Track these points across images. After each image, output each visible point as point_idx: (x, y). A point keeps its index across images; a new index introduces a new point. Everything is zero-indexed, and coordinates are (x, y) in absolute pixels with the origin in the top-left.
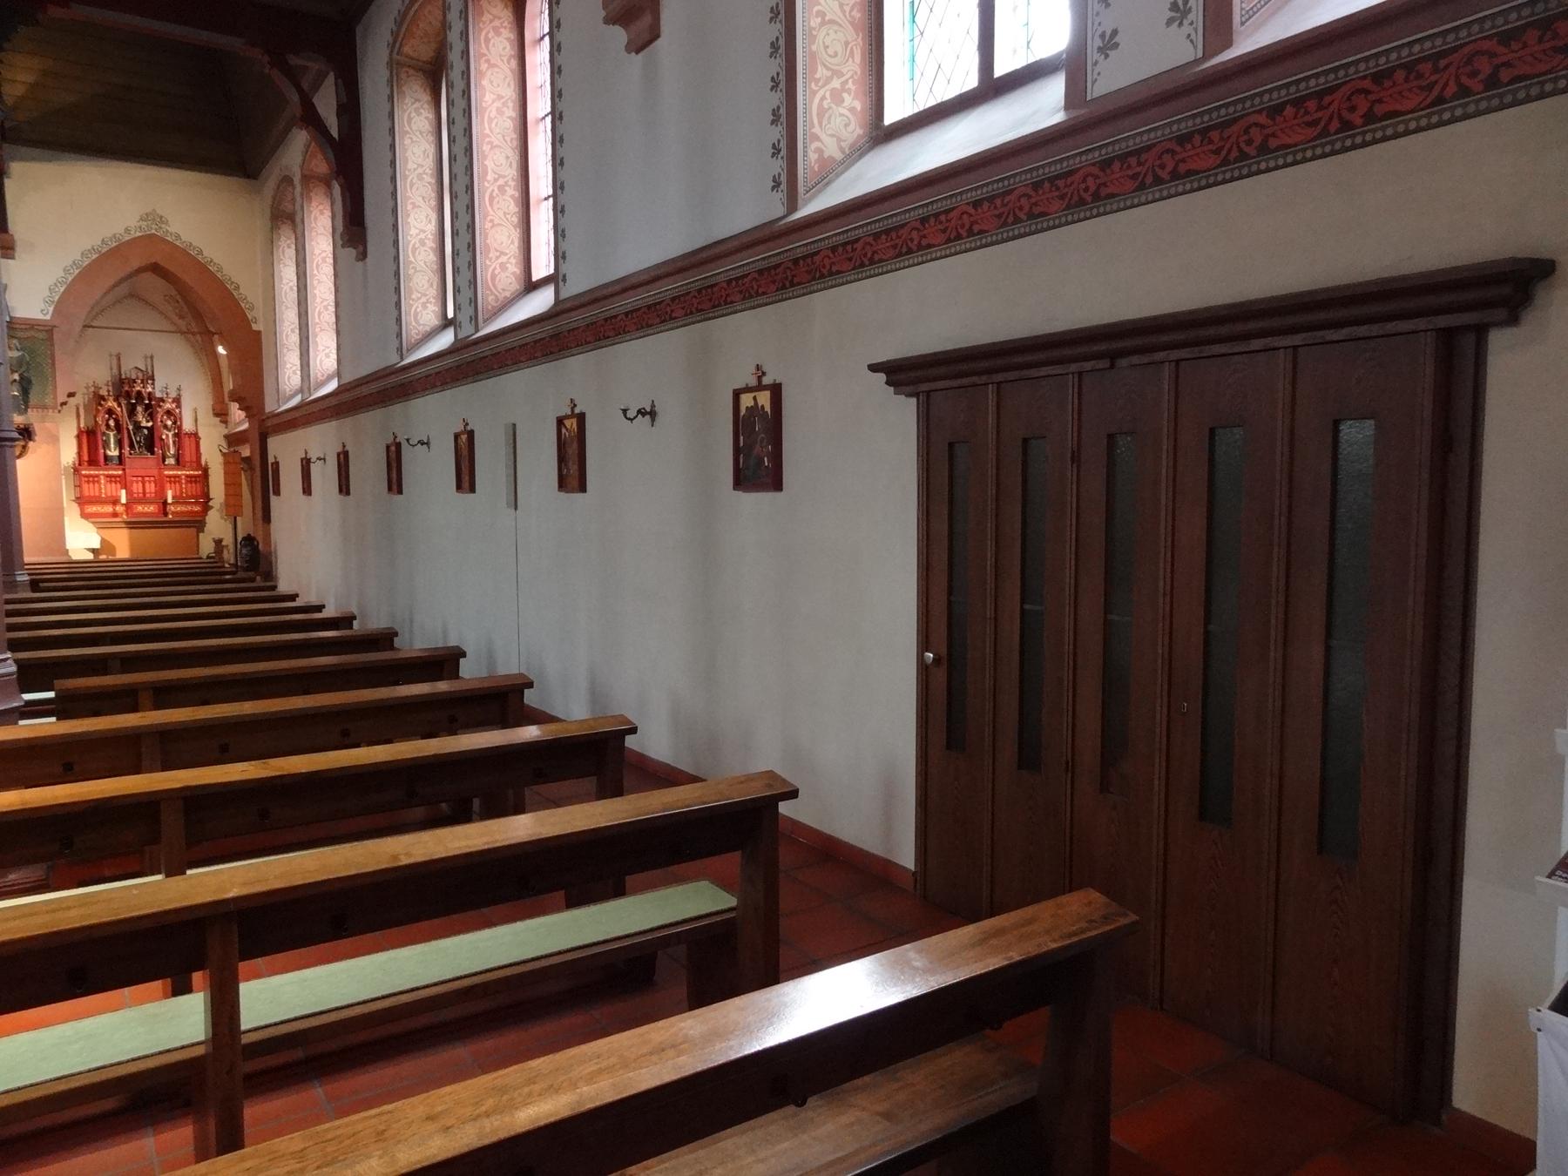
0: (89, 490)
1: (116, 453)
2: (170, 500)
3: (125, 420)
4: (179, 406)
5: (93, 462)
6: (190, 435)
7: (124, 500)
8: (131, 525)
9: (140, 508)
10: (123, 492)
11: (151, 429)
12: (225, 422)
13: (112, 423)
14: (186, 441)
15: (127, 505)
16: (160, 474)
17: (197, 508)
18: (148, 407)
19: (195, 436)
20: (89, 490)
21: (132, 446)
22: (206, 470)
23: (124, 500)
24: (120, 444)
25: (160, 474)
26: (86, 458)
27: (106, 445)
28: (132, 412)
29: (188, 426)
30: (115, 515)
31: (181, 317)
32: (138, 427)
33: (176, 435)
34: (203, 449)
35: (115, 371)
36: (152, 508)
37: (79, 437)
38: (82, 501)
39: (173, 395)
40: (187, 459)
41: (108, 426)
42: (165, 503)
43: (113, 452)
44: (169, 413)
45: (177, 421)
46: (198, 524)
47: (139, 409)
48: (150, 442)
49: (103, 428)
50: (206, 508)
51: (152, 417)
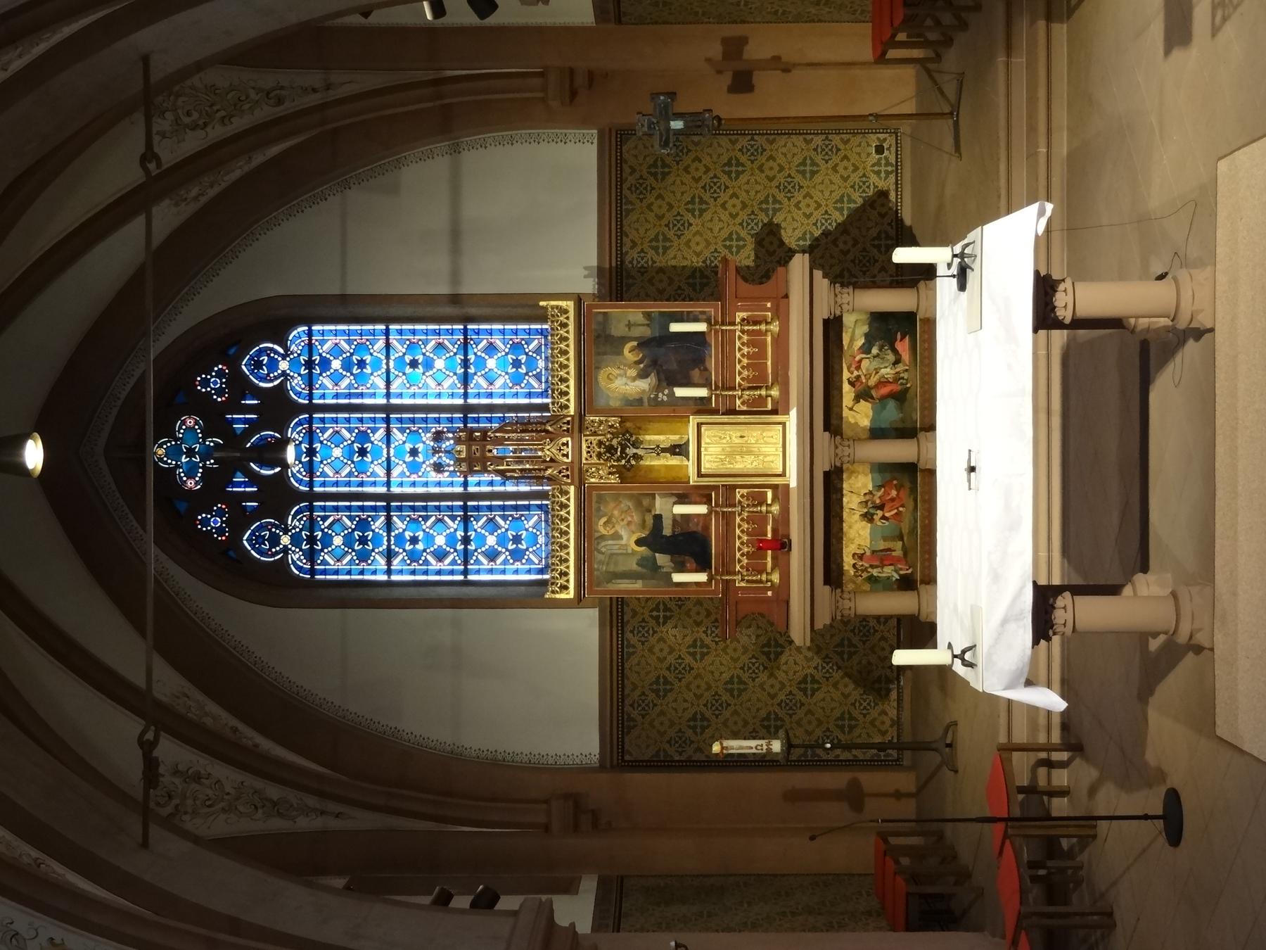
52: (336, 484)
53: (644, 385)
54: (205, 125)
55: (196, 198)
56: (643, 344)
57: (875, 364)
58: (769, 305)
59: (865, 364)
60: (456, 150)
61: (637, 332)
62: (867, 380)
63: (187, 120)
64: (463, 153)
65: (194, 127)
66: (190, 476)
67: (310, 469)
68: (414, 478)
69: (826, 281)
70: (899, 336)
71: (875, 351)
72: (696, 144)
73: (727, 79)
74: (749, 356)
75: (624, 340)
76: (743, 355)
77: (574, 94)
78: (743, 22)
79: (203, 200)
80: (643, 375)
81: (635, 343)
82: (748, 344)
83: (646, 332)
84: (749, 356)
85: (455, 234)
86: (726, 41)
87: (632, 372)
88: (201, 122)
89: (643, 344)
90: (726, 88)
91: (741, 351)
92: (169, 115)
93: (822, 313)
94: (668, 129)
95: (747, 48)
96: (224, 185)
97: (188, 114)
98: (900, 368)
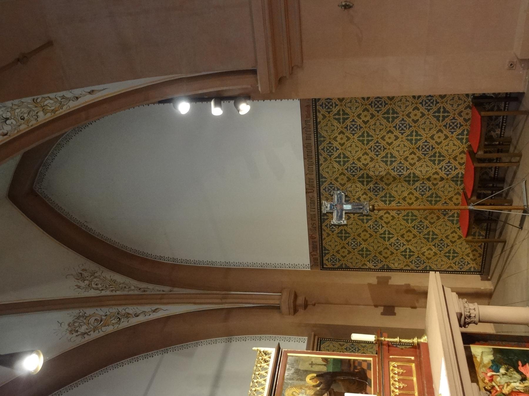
54: (102, 290)
55: (83, 334)
56: (320, 376)
58: (413, 358)
60: (230, 341)
61: (316, 368)
62: (501, 389)
63: (94, 286)
64: (234, 343)
65: (98, 289)
70: (520, 363)
71: (502, 371)
72: (364, 347)
73: (381, 309)
76: (395, 374)
77: (295, 311)
78: (389, 269)
79: (87, 338)
81: (315, 375)
82: (399, 381)
85: (217, 379)
86: (378, 277)
88: (101, 289)
89: (320, 376)
90: (380, 314)
92: (87, 282)
94: (342, 210)
95: (390, 281)
96: (102, 334)
97: (96, 284)
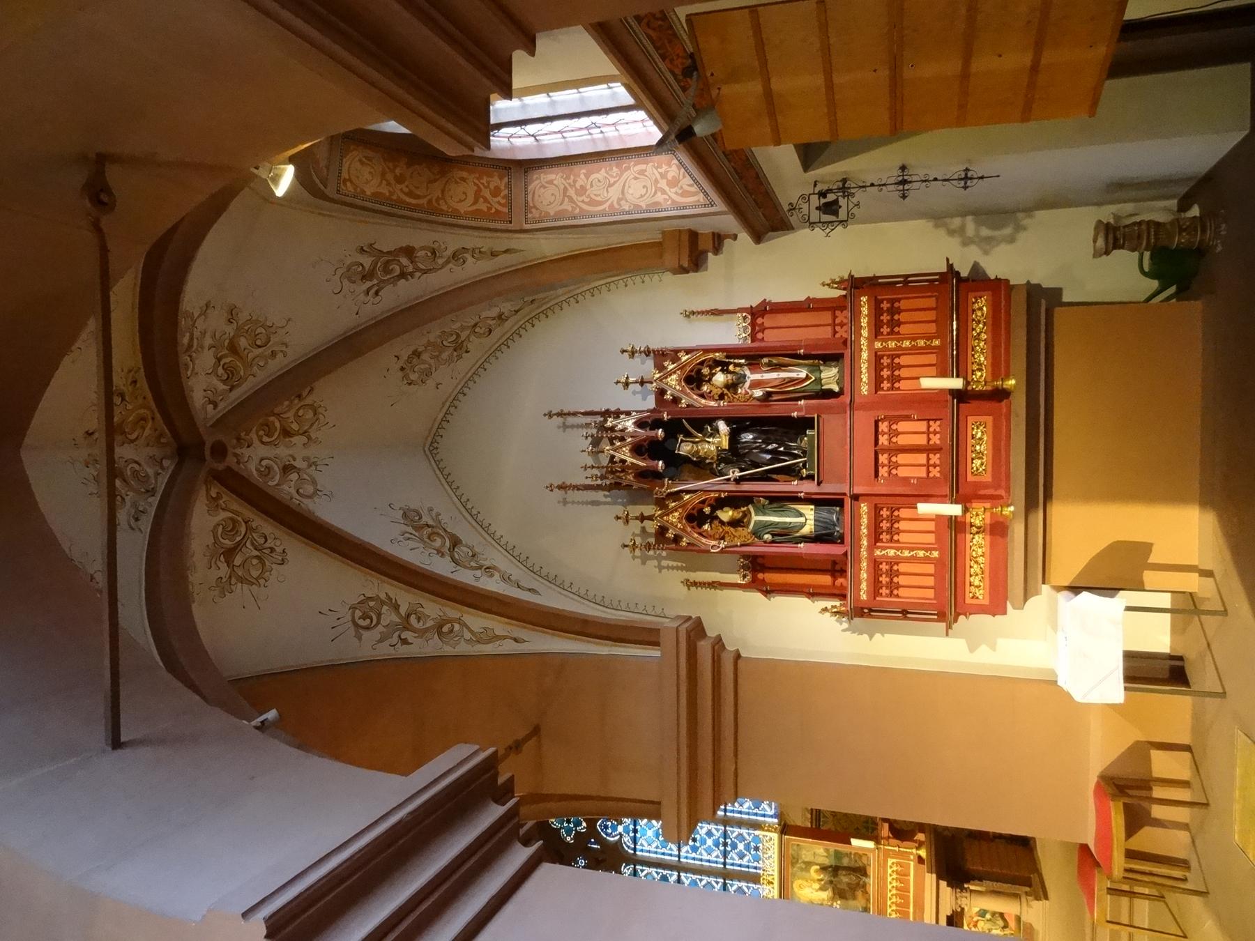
0: (917, 584)
1: (809, 511)
2: (956, 383)
3: (714, 485)
4: (674, 355)
5: (836, 568)
6: (756, 330)
7: (955, 510)
8: (1039, 494)
9: (979, 465)
10: (924, 508)
11: (738, 425)
12: (718, 241)
13: (726, 515)
14: (773, 338)
15: (964, 500)
16: (868, 406)
17: (982, 306)
18: (675, 428)
19: (758, 314)
20: (917, 584)
21: (792, 472)
22: (856, 285)
23: (955, 510)
24: (780, 501)
25: (868, 406)
26: (826, 579)
27: (784, 534)
28: (700, 467)
29: (732, 334)
30: (998, 529)
31: (459, 348)
32: (735, 454)
33: (753, 358)
34: (799, 296)
35: (600, 495)
36: (980, 435)
37: (769, 591)
38: (948, 608)
39: (647, 367)
40: (826, 333)
41: (735, 523)
42: (960, 396)
43: (807, 519)
44: (695, 379)
45: (727, 358)
46: (1036, 313)
47: (685, 449)
48: (777, 433)
49: (743, 533)
50: (978, 281)
51: (703, 423)
52: (649, 852)
53: (825, 895)
57: (988, 926)
59: (981, 924)
66: (569, 832)
67: (635, 841)
68: (694, 855)
69: (949, 889)
74: (897, 889)
75: (809, 864)
80: (822, 889)
83: (827, 862)
84: (897, 889)
87: (817, 886)
89: (824, 869)
91: (892, 883)
93: (946, 911)
98: (1007, 931)
